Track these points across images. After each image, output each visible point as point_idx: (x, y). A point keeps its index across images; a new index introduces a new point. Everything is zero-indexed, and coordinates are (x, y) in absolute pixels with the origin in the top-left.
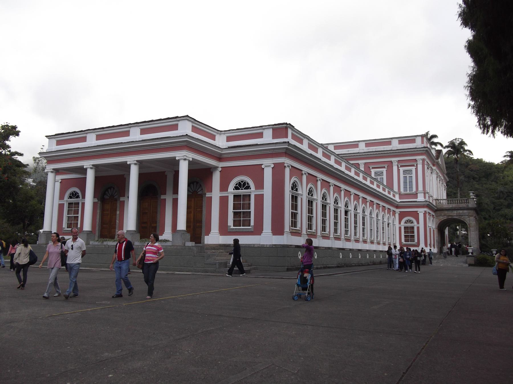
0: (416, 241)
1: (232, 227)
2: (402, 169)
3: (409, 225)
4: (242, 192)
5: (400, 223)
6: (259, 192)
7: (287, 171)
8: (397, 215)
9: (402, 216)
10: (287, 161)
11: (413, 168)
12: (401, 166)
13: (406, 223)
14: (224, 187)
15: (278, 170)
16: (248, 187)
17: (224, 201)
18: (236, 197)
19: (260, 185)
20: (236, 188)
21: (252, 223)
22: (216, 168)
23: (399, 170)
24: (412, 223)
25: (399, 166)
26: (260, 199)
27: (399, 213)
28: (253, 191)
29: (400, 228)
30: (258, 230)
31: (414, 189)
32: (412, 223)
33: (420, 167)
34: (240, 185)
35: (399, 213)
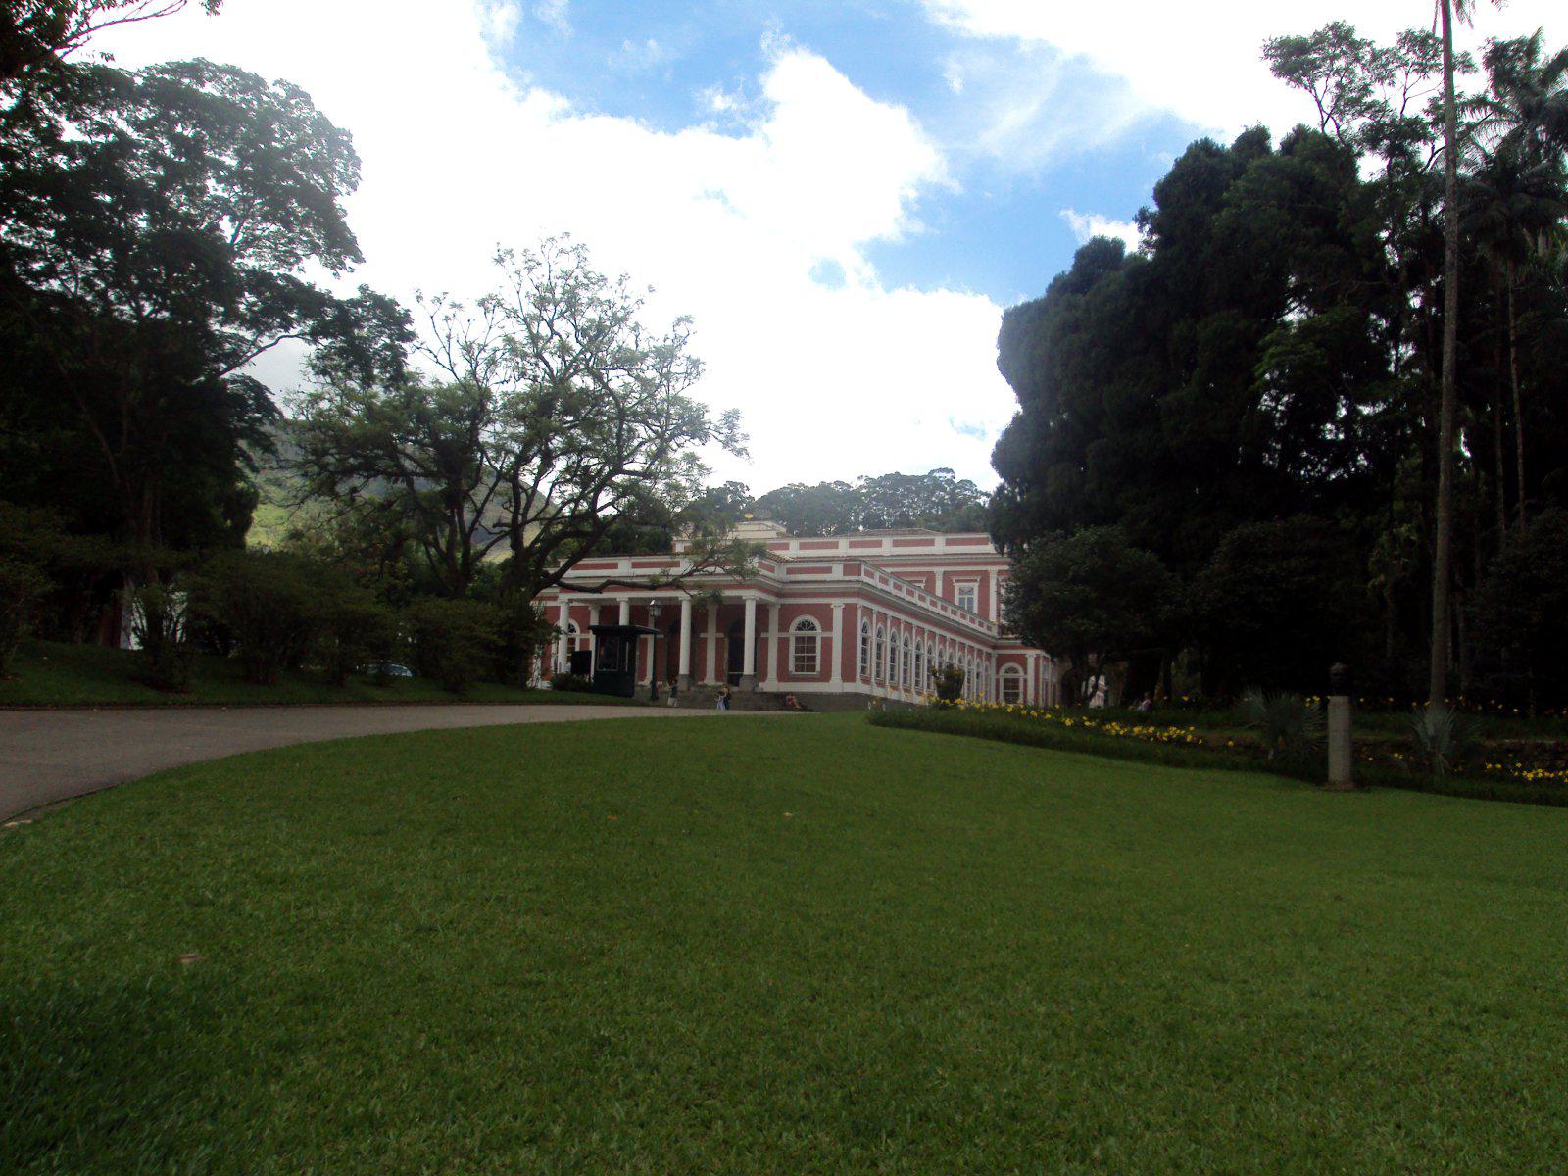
1: (794, 673)
4: (808, 633)
5: (997, 672)
6: (827, 635)
7: (860, 612)
8: (993, 661)
10: (861, 602)
14: (784, 627)
15: (849, 612)
16: (814, 629)
17: (783, 644)
18: (798, 639)
19: (828, 626)
20: (799, 629)
21: (818, 668)
22: (774, 604)
26: (827, 644)
28: (819, 633)
30: (826, 676)
34: (802, 626)
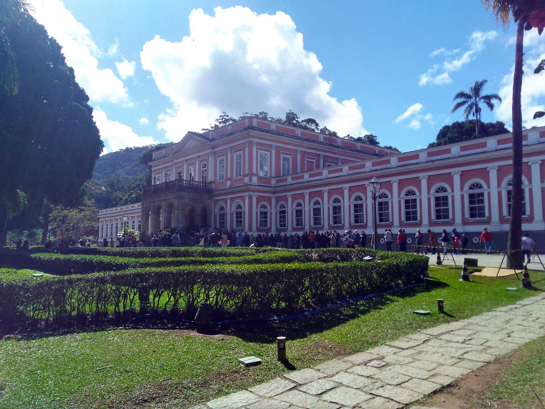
0: (269, 226)
2: (259, 151)
3: (264, 210)
5: (257, 208)
9: (232, 200)
11: (269, 153)
12: (260, 149)
13: (261, 207)
23: (257, 152)
24: (266, 208)
25: (258, 149)
27: (257, 197)
29: (257, 212)
31: (269, 175)
32: (266, 208)
33: (274, 152)
35: (257, 197)
